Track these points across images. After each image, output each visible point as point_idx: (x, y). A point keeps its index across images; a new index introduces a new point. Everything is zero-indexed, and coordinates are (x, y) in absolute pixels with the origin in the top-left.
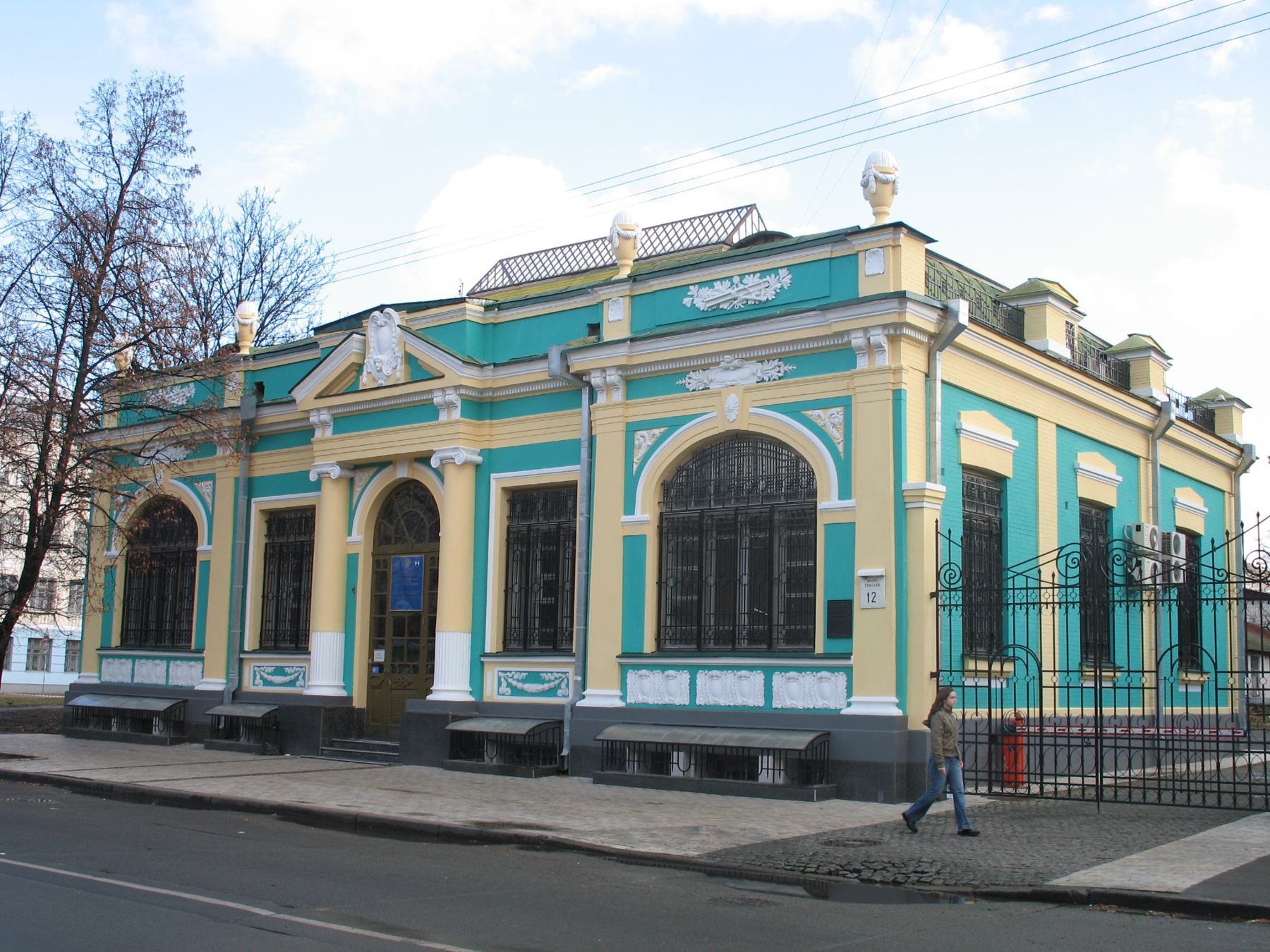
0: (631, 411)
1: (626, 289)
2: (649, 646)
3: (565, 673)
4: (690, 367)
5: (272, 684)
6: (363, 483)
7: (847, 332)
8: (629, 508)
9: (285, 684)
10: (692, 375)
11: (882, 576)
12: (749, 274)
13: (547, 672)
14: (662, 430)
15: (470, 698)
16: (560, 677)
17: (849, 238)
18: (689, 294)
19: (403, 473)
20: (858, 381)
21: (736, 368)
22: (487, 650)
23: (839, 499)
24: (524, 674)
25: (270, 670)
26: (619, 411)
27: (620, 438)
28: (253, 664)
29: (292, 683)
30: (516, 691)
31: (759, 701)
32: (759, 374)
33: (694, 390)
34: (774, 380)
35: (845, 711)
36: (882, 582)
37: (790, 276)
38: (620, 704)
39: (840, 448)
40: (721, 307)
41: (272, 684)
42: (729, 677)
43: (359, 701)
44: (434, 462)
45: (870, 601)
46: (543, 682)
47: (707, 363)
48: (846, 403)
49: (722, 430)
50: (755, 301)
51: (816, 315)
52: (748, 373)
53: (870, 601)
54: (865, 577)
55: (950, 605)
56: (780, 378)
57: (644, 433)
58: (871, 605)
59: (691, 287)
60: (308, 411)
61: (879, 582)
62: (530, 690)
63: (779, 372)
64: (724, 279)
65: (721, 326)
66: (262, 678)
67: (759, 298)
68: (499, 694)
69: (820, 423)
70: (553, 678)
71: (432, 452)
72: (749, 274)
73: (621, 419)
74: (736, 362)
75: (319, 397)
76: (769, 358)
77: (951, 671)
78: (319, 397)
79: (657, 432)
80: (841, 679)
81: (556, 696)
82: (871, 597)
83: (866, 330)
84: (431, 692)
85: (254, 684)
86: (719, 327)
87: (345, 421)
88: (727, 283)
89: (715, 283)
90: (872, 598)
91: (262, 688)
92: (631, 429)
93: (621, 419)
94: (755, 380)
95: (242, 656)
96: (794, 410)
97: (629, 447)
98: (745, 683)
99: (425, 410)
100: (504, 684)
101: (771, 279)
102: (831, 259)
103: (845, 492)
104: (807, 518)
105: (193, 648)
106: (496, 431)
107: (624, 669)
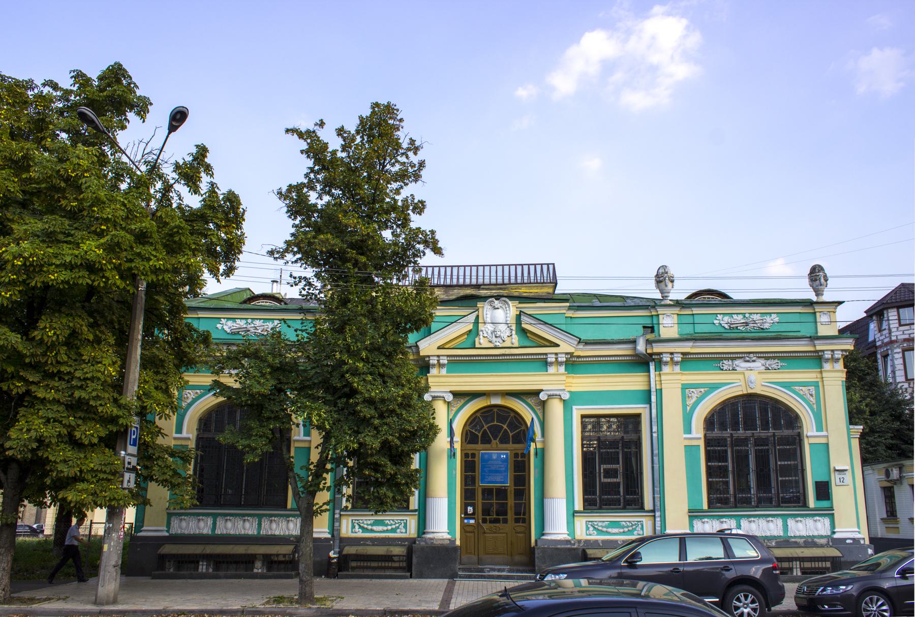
1: (676, 310)
2: (705, 506)
4: (724, 357)
5: (372, 531)
6: (459, 405)
7: (823, 351)
8: (688, 429)
9: (384, 531)
10: (724, 362)
11: (846, 470)
12: (754, 313)
15: (569, 538)
17: (814, 305)
21: (754, 361)
22: (577, 508)
23: (817, 431)
25: (369, 522)
29: (394, 531)
30: (600, 532)
31: (782, 534)
33: (726, 370)
37: (777, 318)
39: (815, 406)
40: (739, 328)
41: (372, 531)
42: (762, 522)
43: (458, 543)
44: (543, 396)
46: (623, 527)
47: (733, 357)
49: (745, 392)
50: (759, 328)
52: (759, 364)
54: (838, 470)
56: (778, 369)
57: (694, 390)
58: (841, 483)
59: (718, 315)
62: (378, 530)
66: (360, 527)
67: (762, 327)
68: (587, 535)
69: (801, 392)
72: (754, 313)
73: (680, 381)
74: (754, 358)
76: (774, 358)
79: (702, 390)
80: (827, 521)
81: (634, 535)
82: (842, 480)
83: (833, 351)
85: (352, 532)
88: (741, 317)
90: (842, 480)
91: (360, 534)
92: (685, 387)
95: (342, 513)
97: (684, 398)
98: (771, 524)
100: (591, 529)
102: (800, 313)
103: (819, 428)
104: (797, 440)
105: (289, 506)
106: (574, 381)
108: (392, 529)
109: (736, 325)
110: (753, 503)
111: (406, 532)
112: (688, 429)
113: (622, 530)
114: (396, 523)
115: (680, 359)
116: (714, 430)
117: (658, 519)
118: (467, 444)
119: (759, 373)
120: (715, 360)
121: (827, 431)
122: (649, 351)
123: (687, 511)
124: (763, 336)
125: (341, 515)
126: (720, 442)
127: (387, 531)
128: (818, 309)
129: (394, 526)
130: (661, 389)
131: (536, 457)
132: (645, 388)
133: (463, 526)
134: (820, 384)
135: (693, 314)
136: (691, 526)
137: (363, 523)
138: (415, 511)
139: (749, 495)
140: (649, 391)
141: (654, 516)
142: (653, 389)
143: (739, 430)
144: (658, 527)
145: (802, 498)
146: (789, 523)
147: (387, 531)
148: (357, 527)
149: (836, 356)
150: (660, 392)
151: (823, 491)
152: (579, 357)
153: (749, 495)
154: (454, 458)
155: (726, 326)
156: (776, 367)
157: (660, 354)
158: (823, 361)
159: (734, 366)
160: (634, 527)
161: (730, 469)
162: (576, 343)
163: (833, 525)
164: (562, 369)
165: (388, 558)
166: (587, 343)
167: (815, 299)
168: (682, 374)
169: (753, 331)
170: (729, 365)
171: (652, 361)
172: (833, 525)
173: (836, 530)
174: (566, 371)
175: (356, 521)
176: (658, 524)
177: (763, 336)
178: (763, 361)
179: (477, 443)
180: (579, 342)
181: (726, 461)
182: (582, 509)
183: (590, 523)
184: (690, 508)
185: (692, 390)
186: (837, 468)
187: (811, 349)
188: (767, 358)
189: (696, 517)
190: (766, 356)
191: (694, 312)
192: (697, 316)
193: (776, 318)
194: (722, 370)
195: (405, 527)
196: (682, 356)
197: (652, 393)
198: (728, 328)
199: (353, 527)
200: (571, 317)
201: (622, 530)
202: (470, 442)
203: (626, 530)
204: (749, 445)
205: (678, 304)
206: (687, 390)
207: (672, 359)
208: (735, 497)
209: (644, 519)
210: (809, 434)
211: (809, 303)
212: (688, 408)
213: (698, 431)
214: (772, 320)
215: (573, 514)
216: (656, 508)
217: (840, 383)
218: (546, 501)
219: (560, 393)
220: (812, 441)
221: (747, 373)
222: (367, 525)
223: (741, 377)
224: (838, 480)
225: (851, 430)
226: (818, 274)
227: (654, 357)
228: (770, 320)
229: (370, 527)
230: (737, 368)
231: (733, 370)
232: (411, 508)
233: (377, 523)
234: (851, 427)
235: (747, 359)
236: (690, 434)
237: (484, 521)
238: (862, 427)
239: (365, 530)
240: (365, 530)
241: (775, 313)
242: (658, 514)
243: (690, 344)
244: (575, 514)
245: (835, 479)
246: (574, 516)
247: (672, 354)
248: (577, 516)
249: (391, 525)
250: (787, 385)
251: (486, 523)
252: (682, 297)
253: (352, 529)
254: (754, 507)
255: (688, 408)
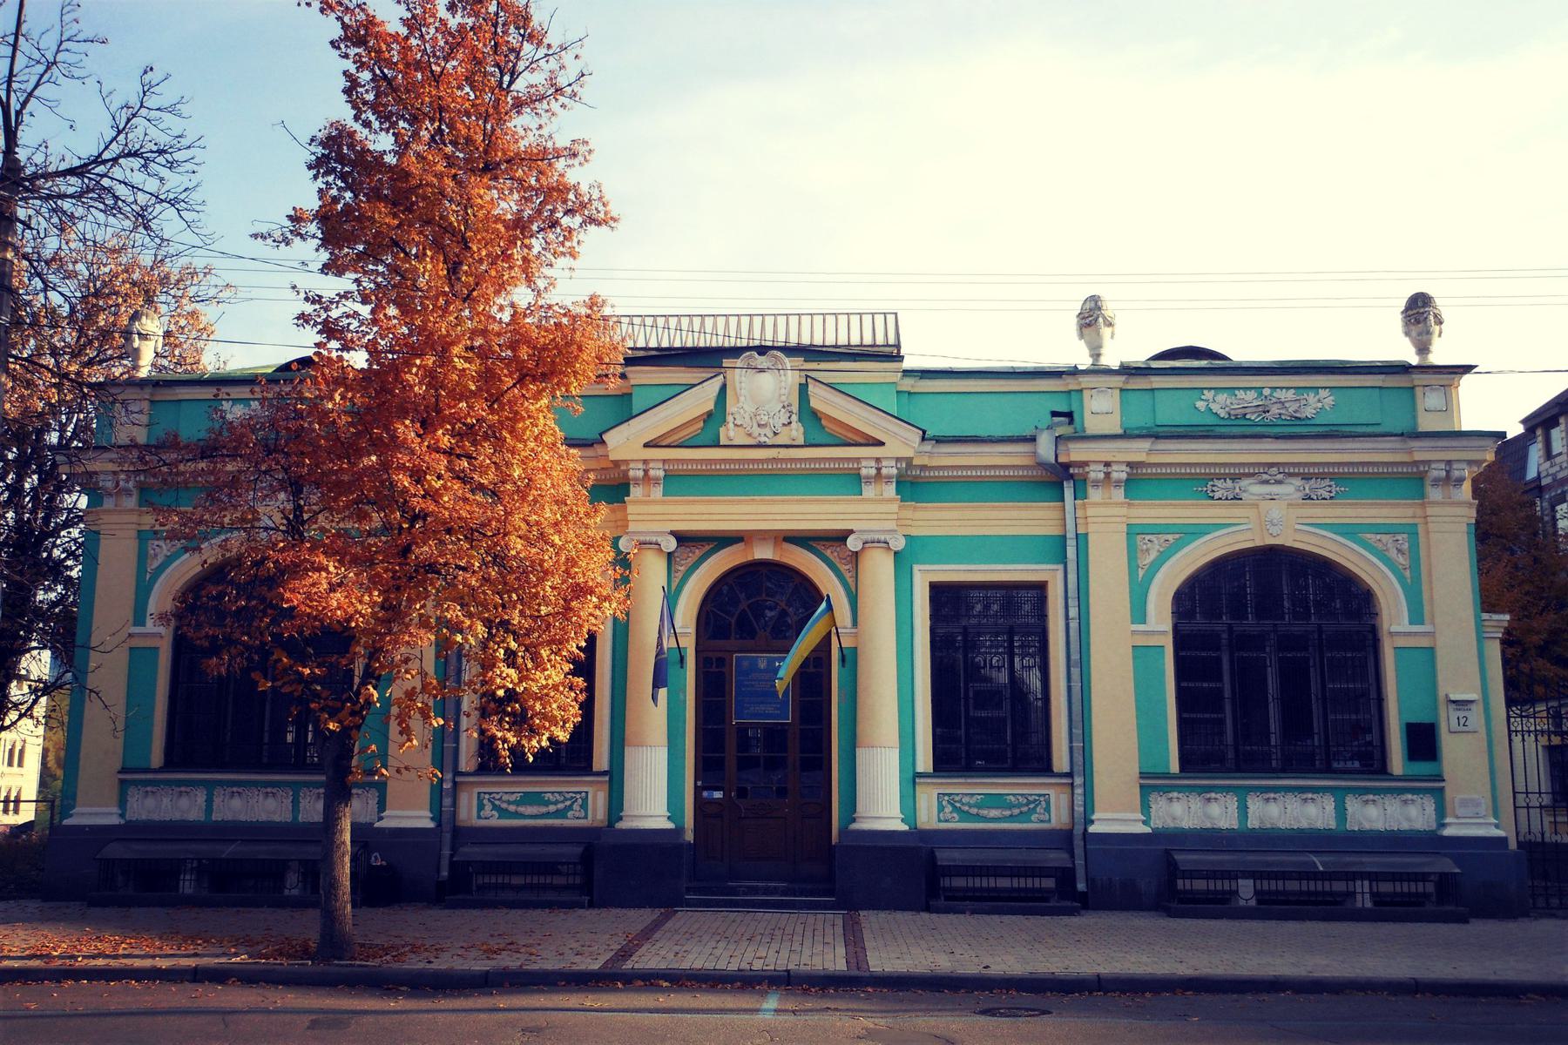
0: (1134, 512)
1: (1118, 381)
2: (1174, 767)
3: (1044, 795)
4: (1215, 474)
5: (517, 815)
6: (690, 561)
8: (1139, 614)
10: (1219, 483)
11: (1472, 702)
12: (1281, 388)
13: (1014, 795)
14: (1177, 536)
15: (906, 828)
16: (1036, 800)
18: (1203, 397)
19: (764, 552)
20: (1430, 511)
21: (1279, 482)
22: (920, 769)
23: (1411, 623)
24: (979, 797)
25: (512, 798)
26: (1124, 511)
27: (1120, 540)
28: (476, 790)
30: (966, 816)
31: (1333, 825)
32: (1307, 491)
34: (1324, 499)
35: (377, 825)
36: (1473, 707)
37: (1331, 398)
38: (1147, 830)
40: (1248, 417)
41: (517, 815)
43: (689, 836)
44: (853, 544)
45: (1462, 723)
46: (1011, 806)
48: (1412, 531)
49: (1259, 543)
51: (1396, 441)
52: (1291, 489)
53: (1462, 723)
54: (1454, 702)
55: (1523, 731)
56: (1331, 498)
59: (1205, 392)
60: (626, 462)
61: (1469, 707)
63: (1330, 492)
64: (1250, 389)
65: (1277, 437)
66: (495, 807)
67: (1298, 415)
68: (940, 821)
70: (1025, 801)
71: (851, 532)
72: (1281, 388)
73: (1124, 519)
74: (1280, 477)
75: (646, 445)
76: (1321, 476)
77: (1540, 793)
78: (646, 445)
79: (1170, 537)
81: (1032, 822)
82: (1462, 721)
83: (1449, 462)
84: (854, 820)
85: (479, 817)
86: (1277, 438)
87: (678, 480)
88: (1251, 395)
89: (1237, 392)
91: (496, 821)
92: (1133, 532)
93: (1124, 519)
94: (1300, 495)
95: (458, 779)
96: (1349, 531)
97: (1132, 553)
99: (852, 480)
100: (949, 809)
101: (1312, 398)
102: (1380, 388)
103: (1417, 616)
104: (1369, 641)
106: (919, 515)
107: (1145, 790)
108: (557, 811)
109: (1243, 411)
110: (1274, 763)
111: (586, 817)
112: (1139, 614)
113: (1007, 813)
114: (566, 799)
115: (1124, 476)
116: (1195, 618)
117: (1079, 791)
118: (709, 638)
119: (1289, 505)
120: (1200, 482)
121: (1433, 624)
122: (1062, 459)
123: (1138, 775)
124: (1297, 430)
125: (455, 784)
126: (1209, 641)
127: (542, 816)
128: (1418, 379)
129: (561, 806)
130: (1087, 534)
131: (843, 666)
132: (1056, 531)
133: (700, 804)
134: (1421, 529)
135: (1153, 390)
136: (1145, 807)
137: (500, 799)
138: (604, 773)
139: (1266, 748)
140: (1064, 537)
141: (1072, 784)
142: (1071, 535)
143: (1247, 619)
144: (1078, 806)
145: (1377, 755)
146: (1348, 805)
147: (542, 816)
148: (488, 807)
149: (1456, 474)
150: (1082, 540)
151: (1423, 741)
152: (923, 468)
153: (1266, 748)
154: (682, 667)
155: (1223, 414)
156: (1326, 495)
157: (1085, 464)
158: (1428, 482)
159: (1237, 490)
160: (1032, 806)
161: (1227, 693)
162: (918, 439)
163: (1441, 811)
164: (890, 490)
165: (550, 868)
166: (940, 440)
167: (1414, 360)
168: (1129, 504)
169: (1280, 422)
170: (1227, 489)
171: (1067, 479)
172: (1441, 811)
173: (1447, 820)
174: (898, 492)
175: (487, 796)
176: (1079, 800)
177: (1297, 430)
178: (1298, 482)
179: (727, 637)
180: (923, 439)
181: (1220, 679)
182: (931, 770)
183: (946, 798)
184: (1144, 770)
185: (1148, 537)
186: (1453, 697)
187: (1405, 458)
188: (1306, 477)
189: (1155, 788)
190: (1306, 474)
191: (1155, 386)
192: (1162, 393)
193: (1328, 399)
194: (1212, 498)
195: (584, 806)
196: (1128, 470)
197: (1068, 542)
198: (1227, 416)
199: (481, 807)
200: (909, 393)
201: (1007, 813)
202: (714, 637)
203: (1016, 811)
204: (1268, 649)
205: (1128, 370)
206: (1139, 537)
207: (1108, 475)
208: (1237, 751)
209: (1052, 792)
210: (1394, 628)
211: (1403, 369)
212: (1141, 573)
213: (1160, 619)
214: (1319, 401)
215: (913, 779)
216: (1076, 769)
217: (1465, 528)
218: (860, 752)
219: (888, 537)
220: (1401, 642)
221: (1264, 505)
222: (509, 803)
223: (1252, 513)
224: (1454, 722)
225: (1486, 623)
226: (1422, 310)
227: (1071, 471)
228: (1318, 403)
229: (512, 808)
230: (1244, 495)
231: (1235, 498)
232: (596, 768)
233: (529, 799)
234: (1485, 616)
235: (1265, 477)
236: (1144, 622)
237: (742, 793)
238: (1507, 617)
239: (504, 813)
240: (504, 813)
241: (1326, 388)
242: (1078, 781)
243: (1145, 445)
244: (917, 780)
245: (1447, 721)
246: (914, 783)
247: (1107, 464)
248: (920, 783)
249: (556, 803)
250: (1349, 531)
251: (745, 797)
252: (1139, 355)
253: (479, 811)
254: (1274, 771)
255: (1141, 573)
